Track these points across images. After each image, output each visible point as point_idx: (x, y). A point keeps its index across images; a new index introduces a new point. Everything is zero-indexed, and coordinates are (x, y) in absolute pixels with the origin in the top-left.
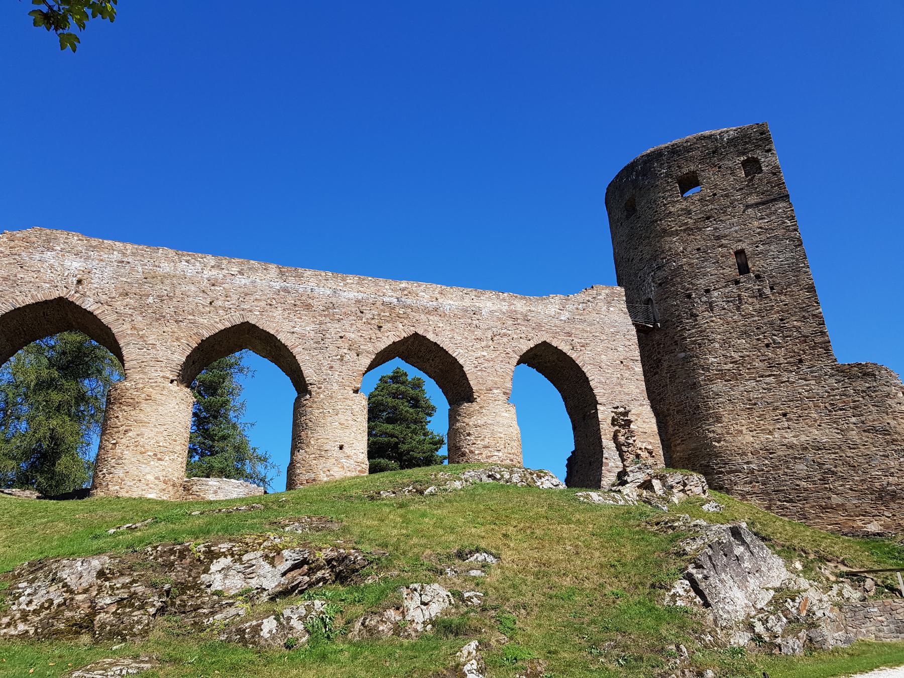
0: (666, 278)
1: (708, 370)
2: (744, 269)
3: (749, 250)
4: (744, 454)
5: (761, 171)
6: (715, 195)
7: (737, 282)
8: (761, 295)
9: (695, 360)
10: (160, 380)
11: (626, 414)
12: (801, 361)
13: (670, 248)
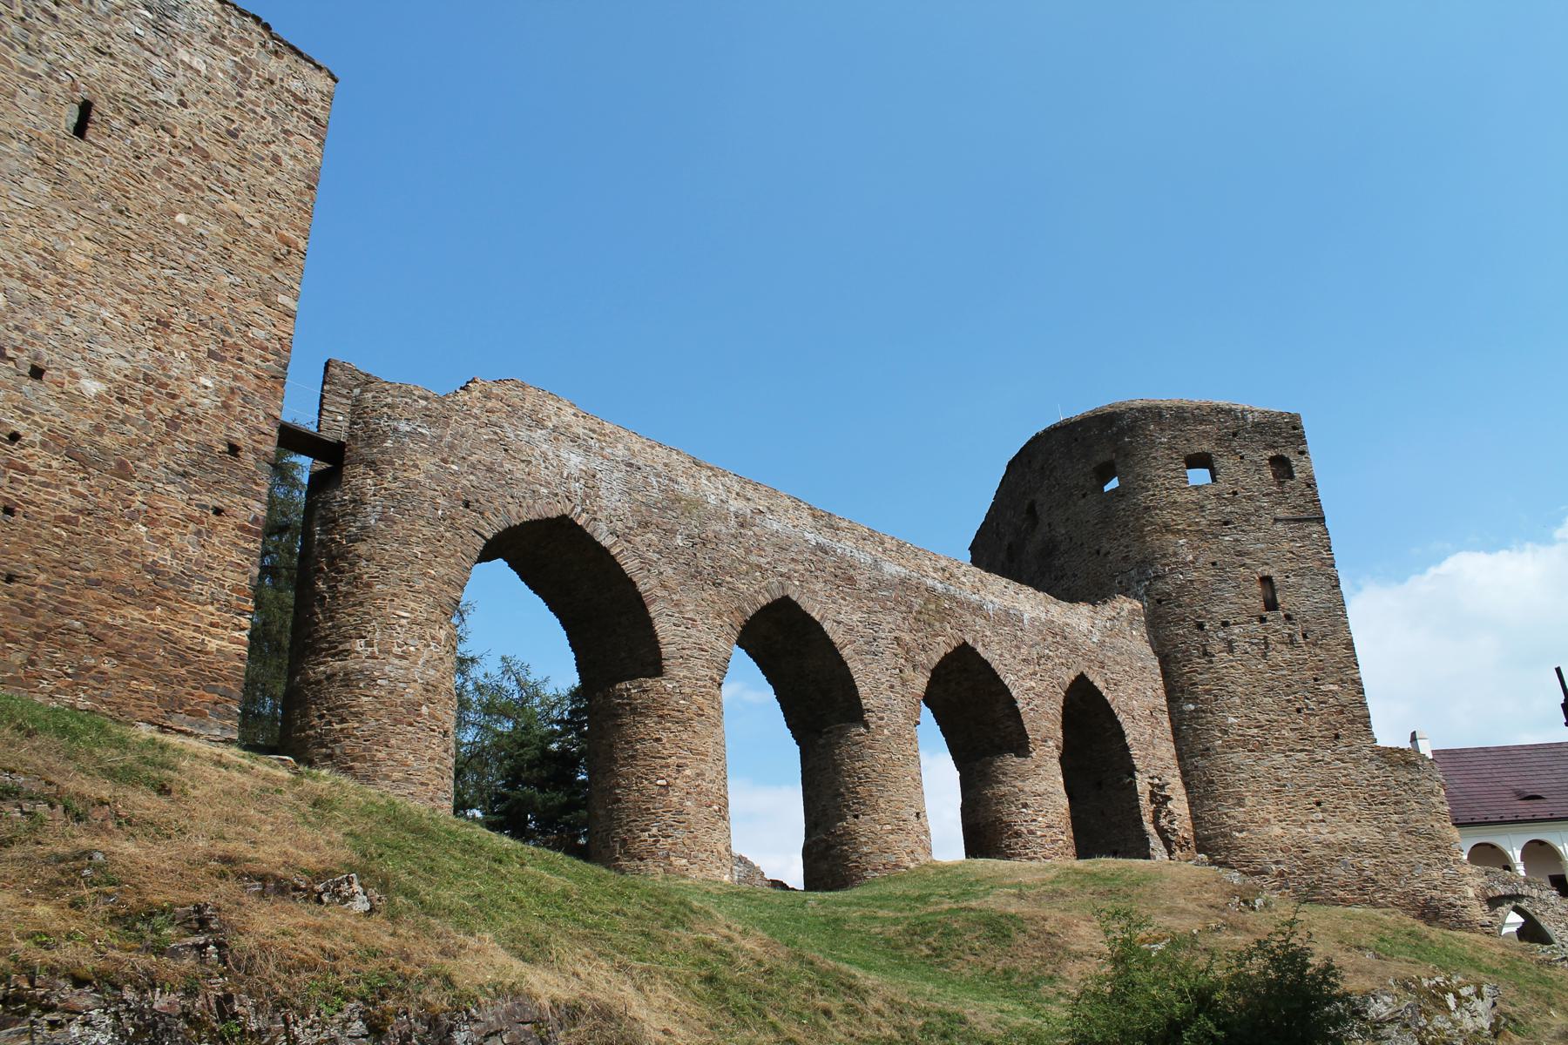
0: (1169, 594)
1: (1226, 732)
2: (1271, 605)
3: (1278, 578)
4: (1272, 850)
5: (1292, 477)
6: (1235, 493)
7: (1262, 620)
8: (1291, 641)
9: (1210, 717)
10: (709, 683)
11: (1162, 787)
12: (1337, 737)
13: (1175, 554)
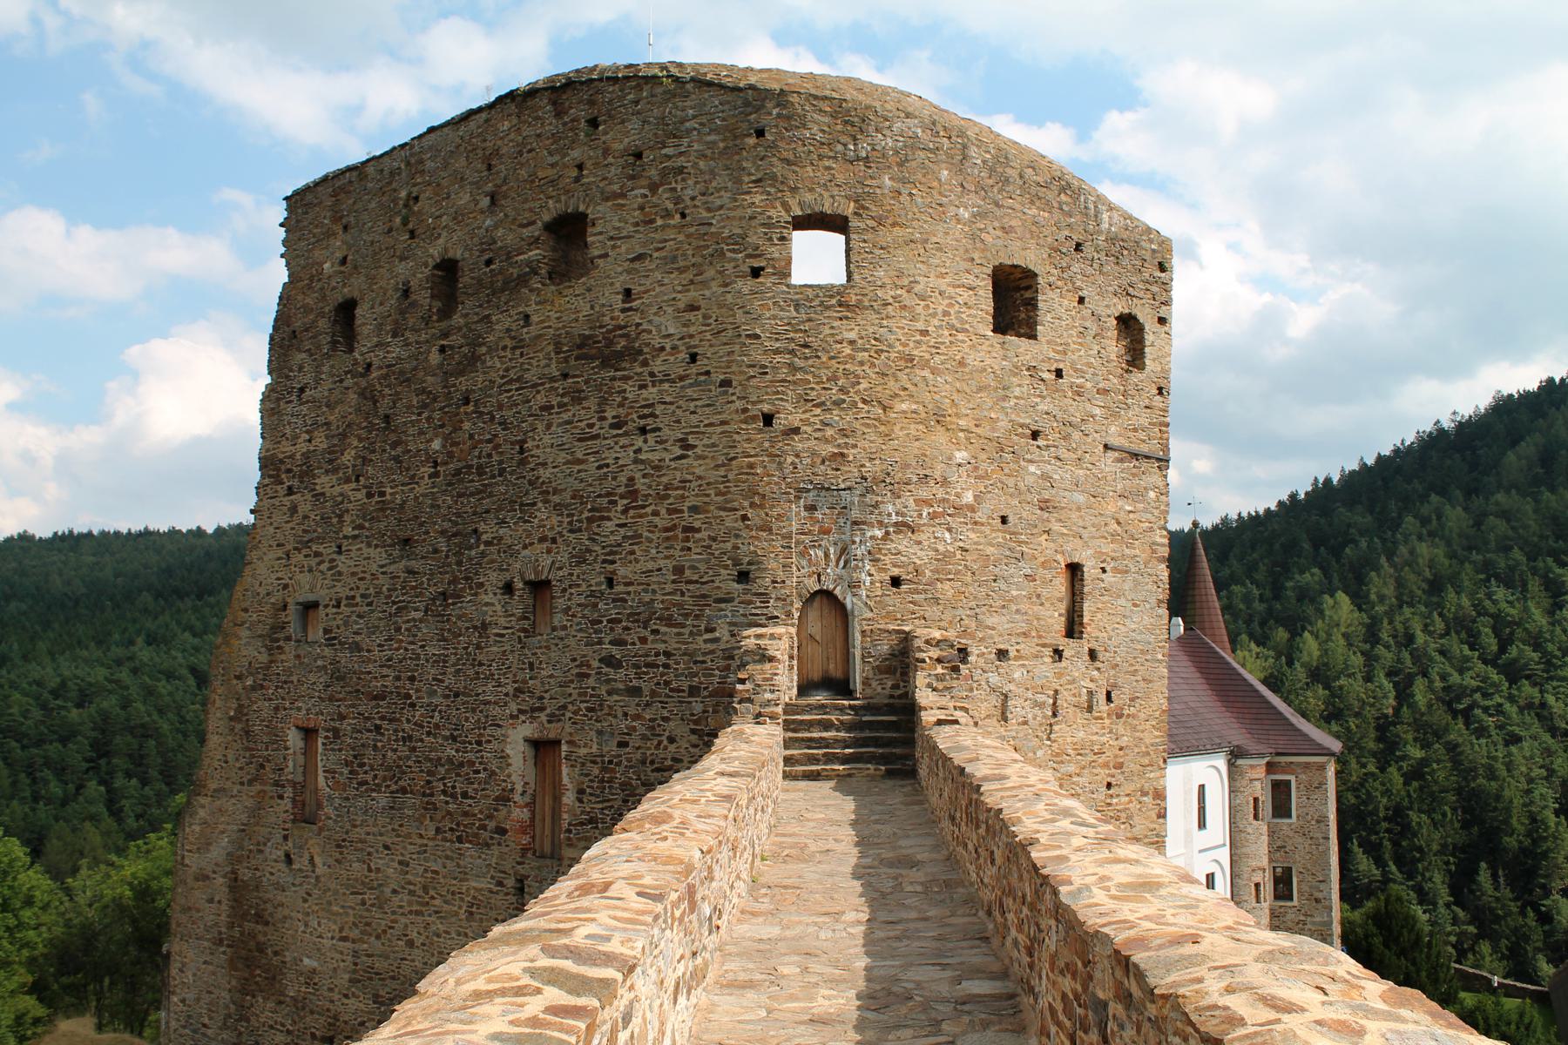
2: (1073, 628)
3: (1090, 571)
7: (1058, 654)
13: (945, 482)
